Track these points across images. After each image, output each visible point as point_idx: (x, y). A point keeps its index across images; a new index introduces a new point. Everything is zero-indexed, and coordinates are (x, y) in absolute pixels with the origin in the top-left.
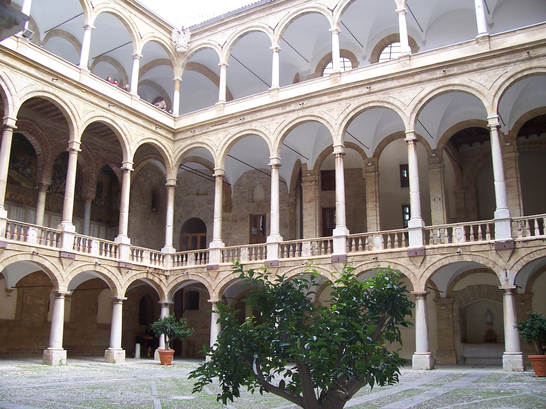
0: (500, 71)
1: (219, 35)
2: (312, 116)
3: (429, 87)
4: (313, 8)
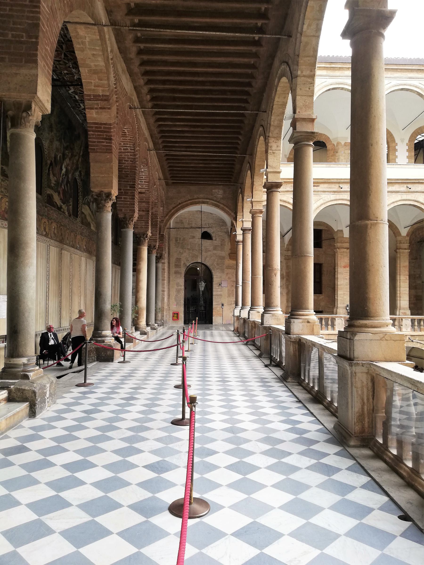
2: (415, 201)
4: (416, 87)
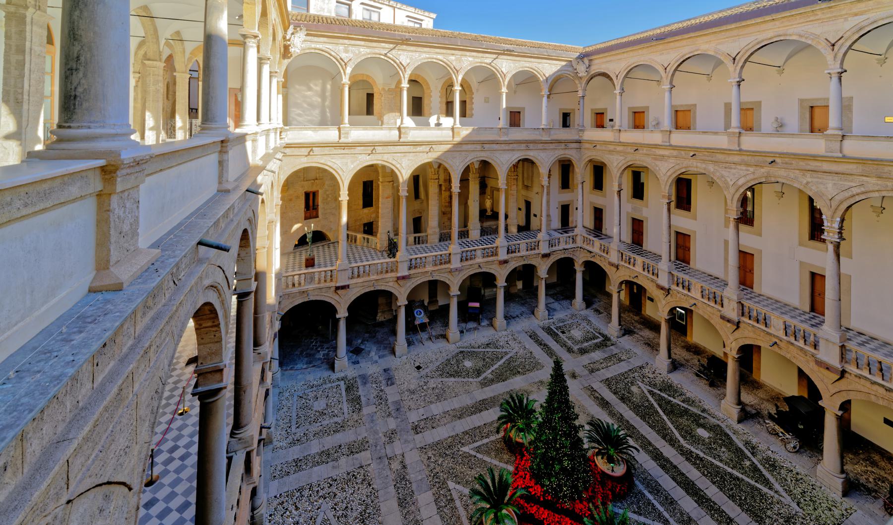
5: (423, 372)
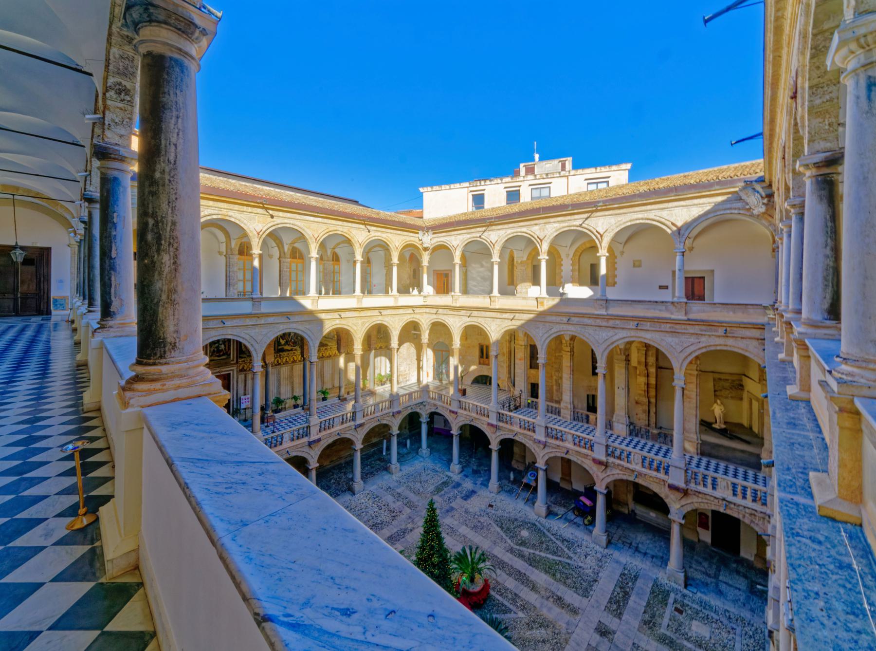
0: (693, 339)
1: (453, 237)
3: (622, 334)
5: (489, 510)
